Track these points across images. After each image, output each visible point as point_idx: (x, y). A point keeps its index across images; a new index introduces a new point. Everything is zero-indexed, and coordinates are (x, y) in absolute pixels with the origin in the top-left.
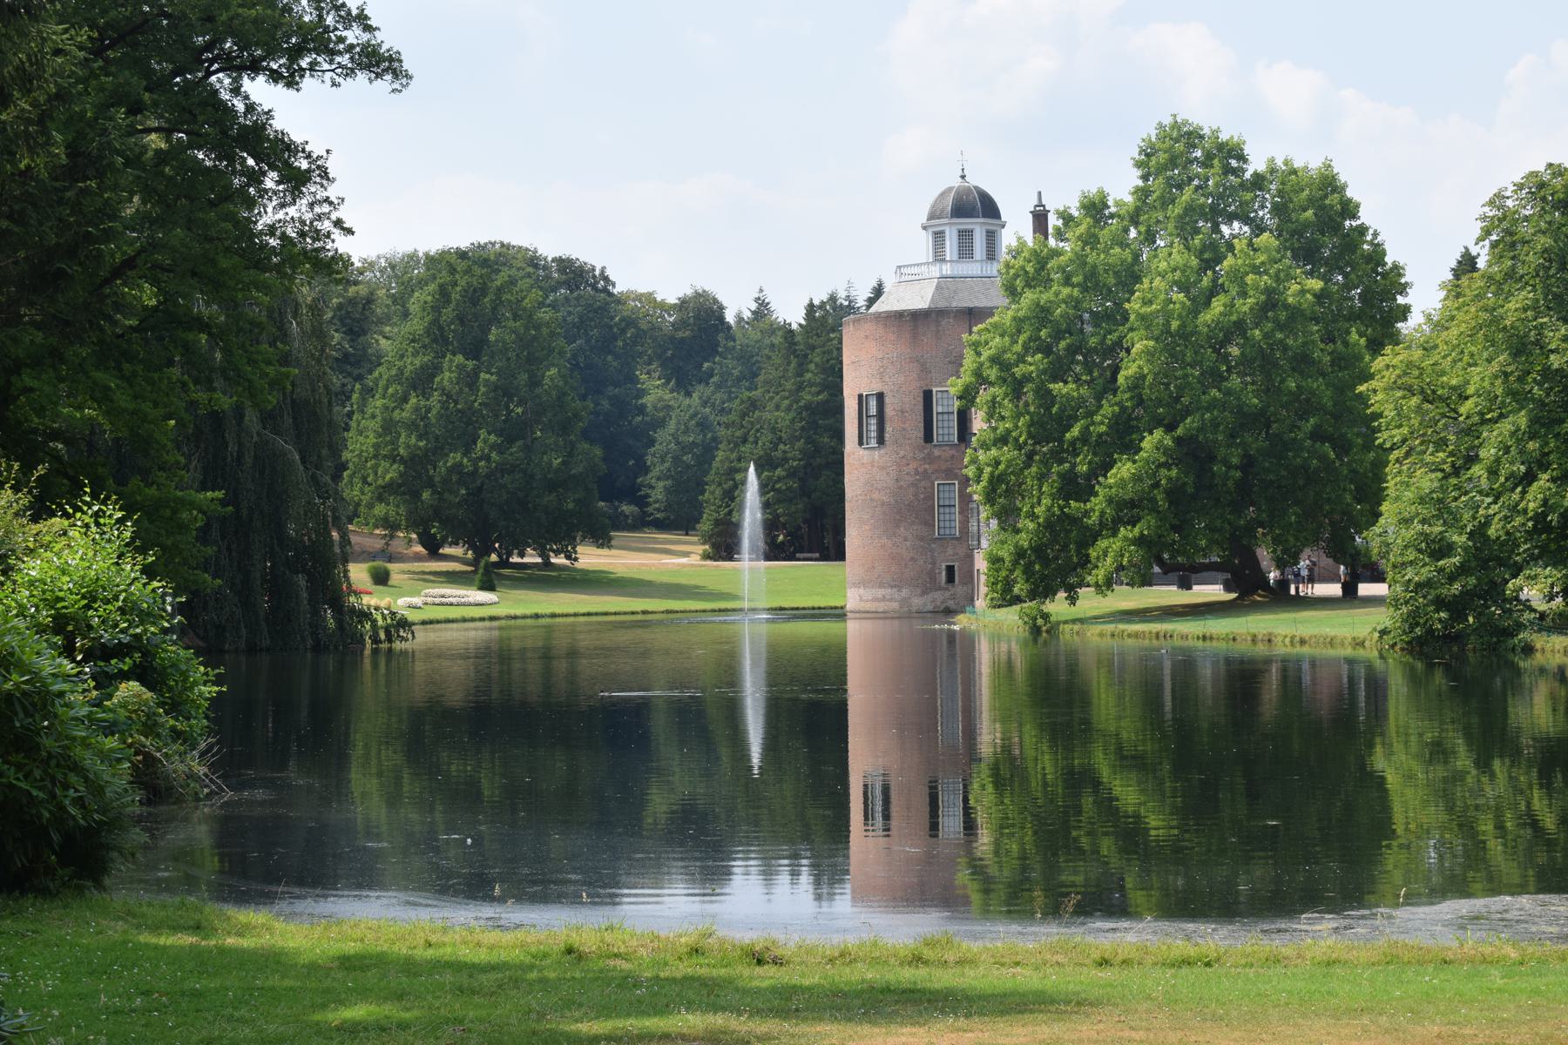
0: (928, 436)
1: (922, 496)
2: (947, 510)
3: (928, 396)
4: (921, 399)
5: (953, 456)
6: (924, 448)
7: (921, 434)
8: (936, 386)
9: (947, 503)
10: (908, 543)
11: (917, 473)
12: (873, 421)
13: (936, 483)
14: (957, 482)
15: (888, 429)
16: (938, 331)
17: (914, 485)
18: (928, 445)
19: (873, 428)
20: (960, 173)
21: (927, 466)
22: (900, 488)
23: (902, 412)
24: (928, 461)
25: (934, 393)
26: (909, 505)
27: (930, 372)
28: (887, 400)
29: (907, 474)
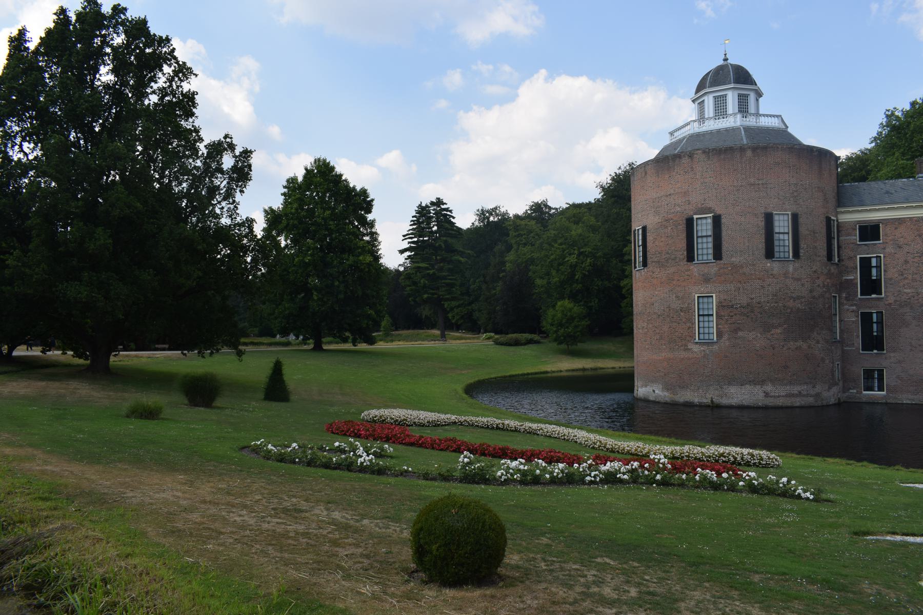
0: (830, 257)
4: (824, 223)
7: (824, 253)
10: (820, 345)
11: (824, 286)
14: (837, 295)
15: (803, 245)
20: (723, 57)
22: (814, 297)
23: (814, 233)
28: (801, 220)
29: (819, 286)
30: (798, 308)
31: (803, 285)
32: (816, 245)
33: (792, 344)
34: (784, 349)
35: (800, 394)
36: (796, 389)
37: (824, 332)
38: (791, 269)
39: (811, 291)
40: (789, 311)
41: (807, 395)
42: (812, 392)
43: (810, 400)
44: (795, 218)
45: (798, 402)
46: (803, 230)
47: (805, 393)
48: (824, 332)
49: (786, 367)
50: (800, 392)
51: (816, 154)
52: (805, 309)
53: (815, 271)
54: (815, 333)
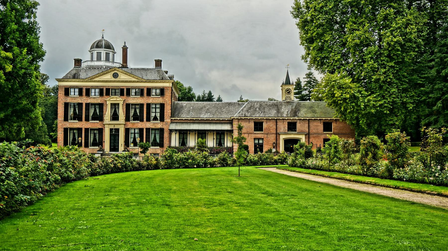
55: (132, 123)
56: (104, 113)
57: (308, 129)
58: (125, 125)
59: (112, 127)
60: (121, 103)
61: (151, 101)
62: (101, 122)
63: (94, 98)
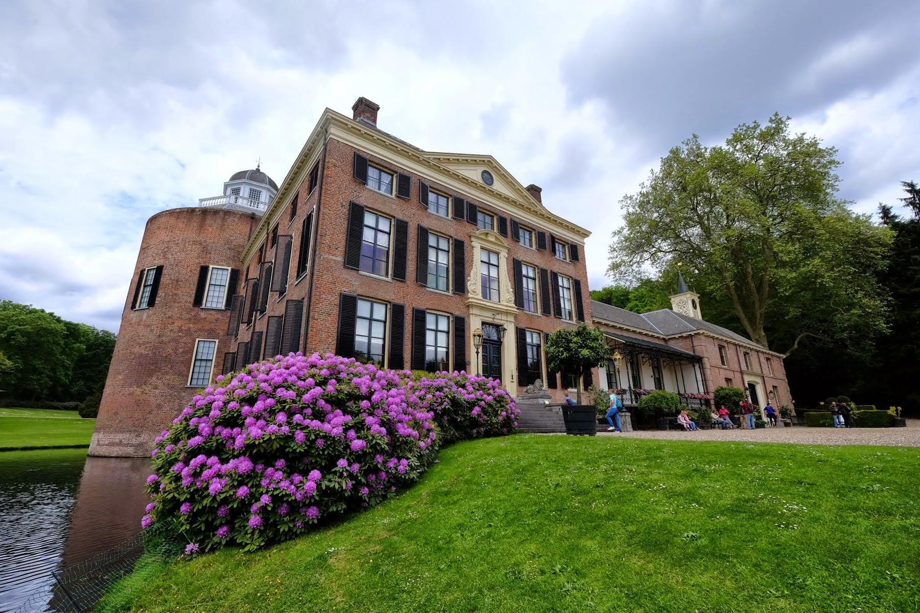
1: (181, 350)
2: (204, 364)
3: (204, 271)
5: (217, 320)
6: (191, 310)
7: (192, 300)
8: (214, 264)
9: (204, 358)
10: (157, 391)
12: (149, 289)
13: (197, 340)
14: (217, 341)
15: (161, 293)
16: (223, 225)
17: (175, 340)
18: (196, 309)
19: (147, 294)
21: (191, 326)
22: (161, 342)
23: (177, 281)
24: (193, 321)
25: (210, 268)
26: (166, 356)
27: (210, 253)
28: (164, 271)
29: (171, 331)
30: (141, 355)
31: (152, 331)
32: (176, 292)
33: (127, 390)
34: (121, 393)
35: (120, 443)
36: (118, 437)
37: (168, 377)
38: (144, 317)
39: (159, 336)
40: (133, 357)
41: (127, 445)
42: (134, 441)
43: (130, 451)
44: (159, 270)
45: (116, 451)
46: (164, 280)
47: (126, 442)
48: (168, 377)
49: (116, 414)
50: (121, 441)
51: (198, 213)
52: (148, 354)
53: (169, 317)
54: (154, 378)
55: (528, 315)
56: (466, 271)
57: (759, 367)
58: (516, 317)
59: (488, 317)
60: (504, 254)
61: (556, 266)
62: (457, 298)
63: (439, 218)
